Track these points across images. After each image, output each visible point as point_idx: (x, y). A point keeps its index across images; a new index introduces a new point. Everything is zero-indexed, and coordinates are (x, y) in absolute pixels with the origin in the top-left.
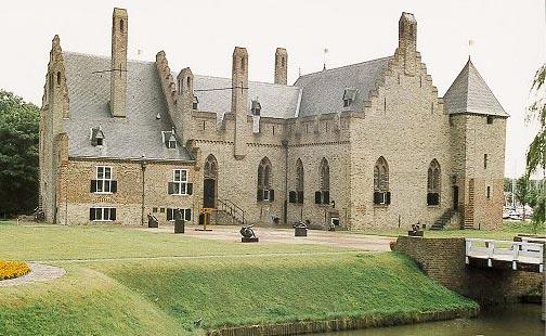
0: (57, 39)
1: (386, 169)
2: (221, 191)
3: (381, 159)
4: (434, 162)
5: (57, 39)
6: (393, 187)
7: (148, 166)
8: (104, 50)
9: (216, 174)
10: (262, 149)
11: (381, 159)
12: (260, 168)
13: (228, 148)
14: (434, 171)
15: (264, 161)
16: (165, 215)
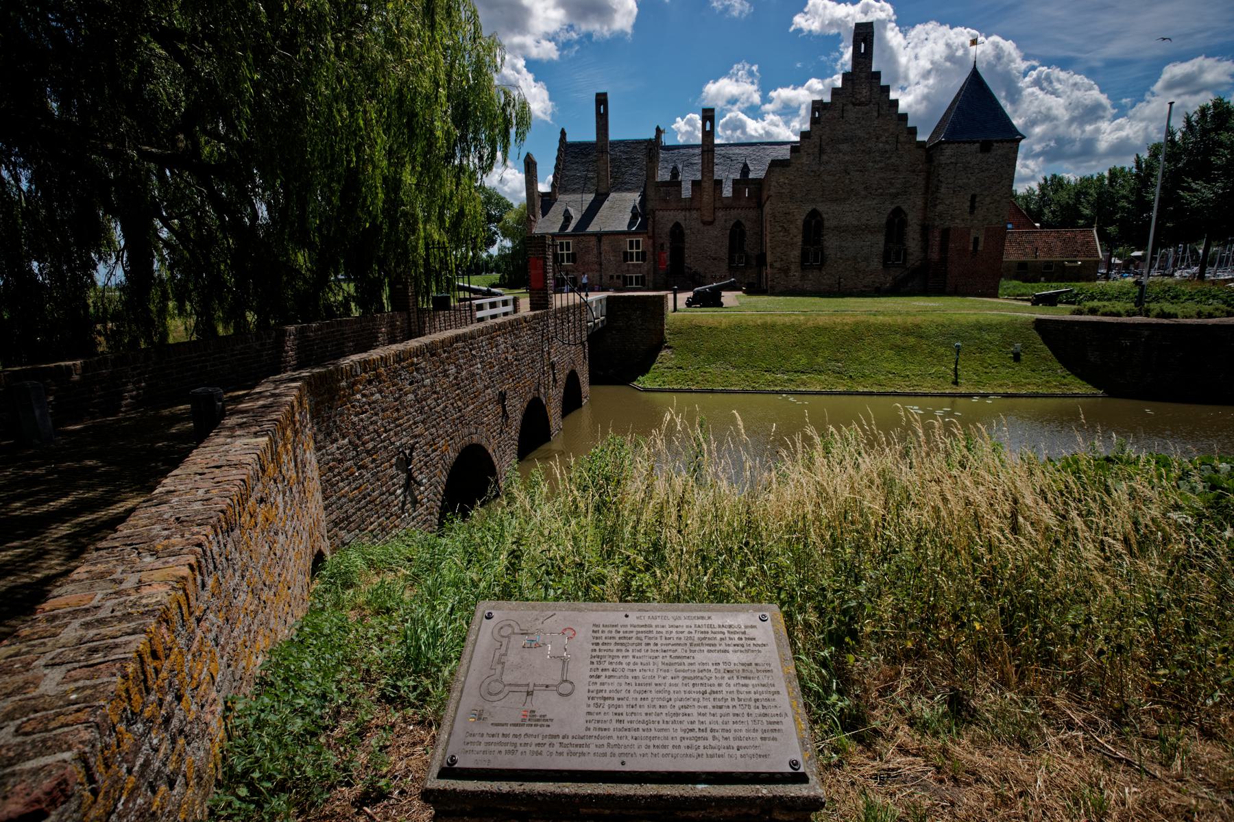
0: (563, 133)
1: (820, 224)
2: (689, 262)
3: (814, 214)
4: (898, 212)
5: (563, 133)
6: (831, 243)
7: (604, 239)
8: (590, 136)
9: (683, 241)
10: (734, 212)
11: (814, 214)
12: (732, 232)
13: (695, 214)
14: (895, 225)
15: (738, 224)
16: (620, 282)
